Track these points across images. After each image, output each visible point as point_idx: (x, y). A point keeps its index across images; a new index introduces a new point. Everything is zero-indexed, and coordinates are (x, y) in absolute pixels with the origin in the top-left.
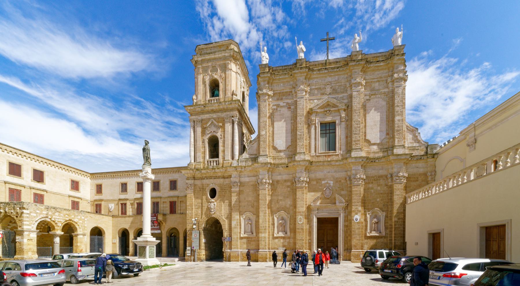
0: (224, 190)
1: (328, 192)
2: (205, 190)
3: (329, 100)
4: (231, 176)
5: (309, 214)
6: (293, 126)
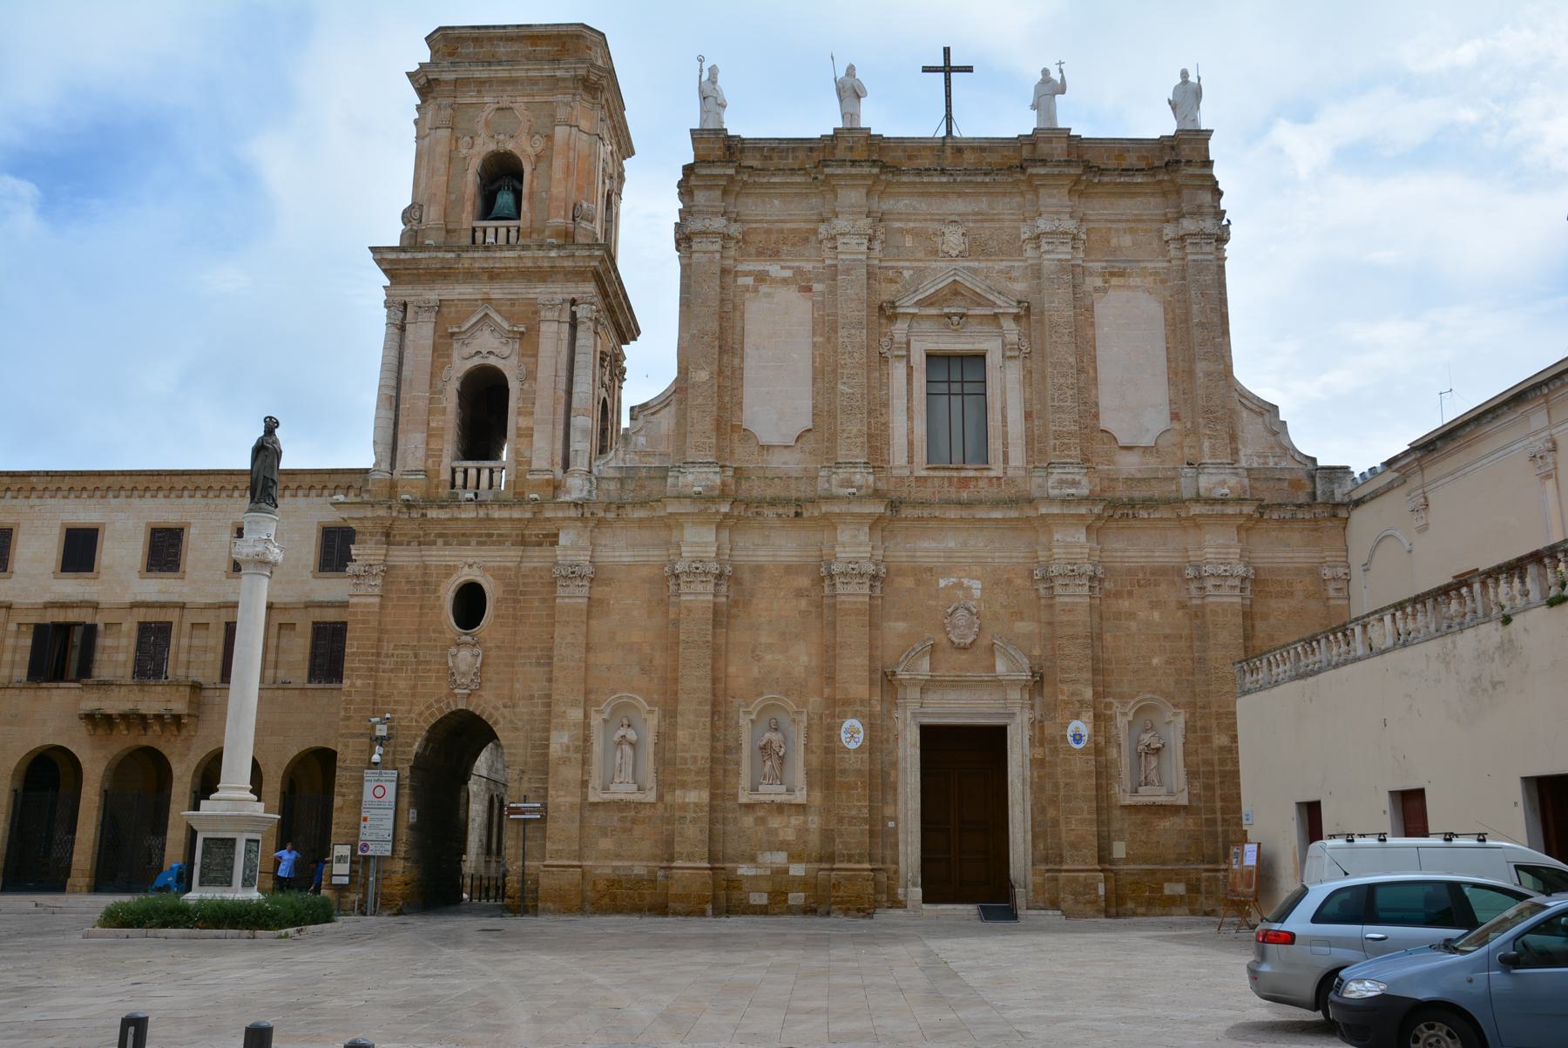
0: (522, 593)
1: (962, 622)
2: (435, 591)
3: (957, 278)
4: (557, 535)
5: (889, 711)
6: (822, 355)
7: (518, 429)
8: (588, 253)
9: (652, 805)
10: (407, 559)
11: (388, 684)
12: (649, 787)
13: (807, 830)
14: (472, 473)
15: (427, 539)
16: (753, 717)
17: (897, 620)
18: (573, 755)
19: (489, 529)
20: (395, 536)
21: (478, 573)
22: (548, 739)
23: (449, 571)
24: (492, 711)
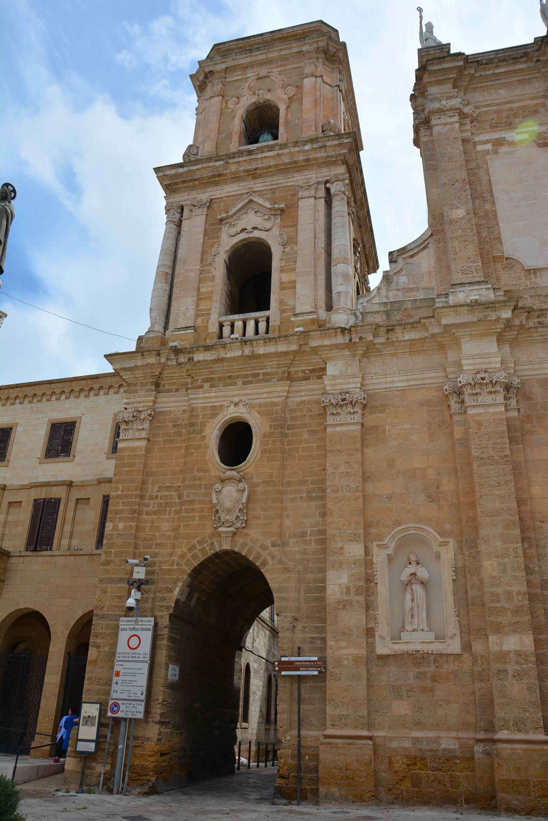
2: (202, 431)
4: (324, 370)
7: (281, 283)
8: (337, 142)
9: (457, 657)
10: (174, 404)
11: (151, 527)
12: (450, 634)
14: (239, 325)
15: (194, 385)
19: (255, 368)
20: (164, 386)
21: (244, 410)
22: (324, 581)
23: (215, 411)
24: (261, 551)
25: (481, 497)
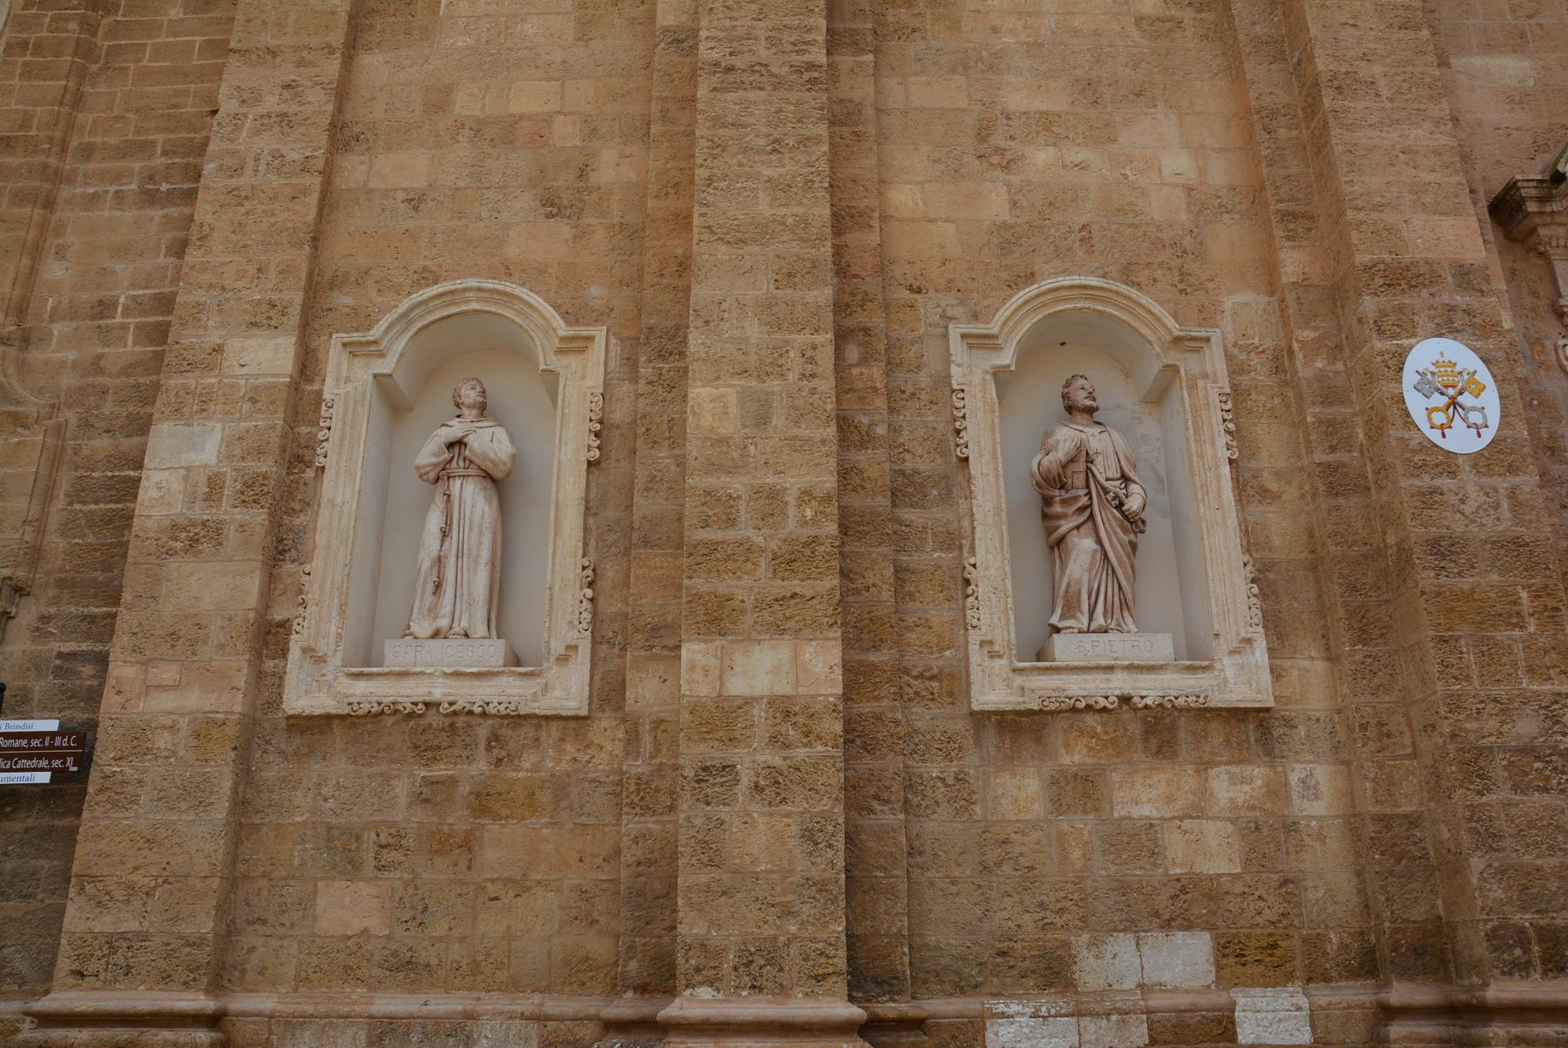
12: (557, 647)
13: (1290, 827)
16: (1006, 358)
17: (1489, 48)
18: (230, 513)
25: (709, 181)
